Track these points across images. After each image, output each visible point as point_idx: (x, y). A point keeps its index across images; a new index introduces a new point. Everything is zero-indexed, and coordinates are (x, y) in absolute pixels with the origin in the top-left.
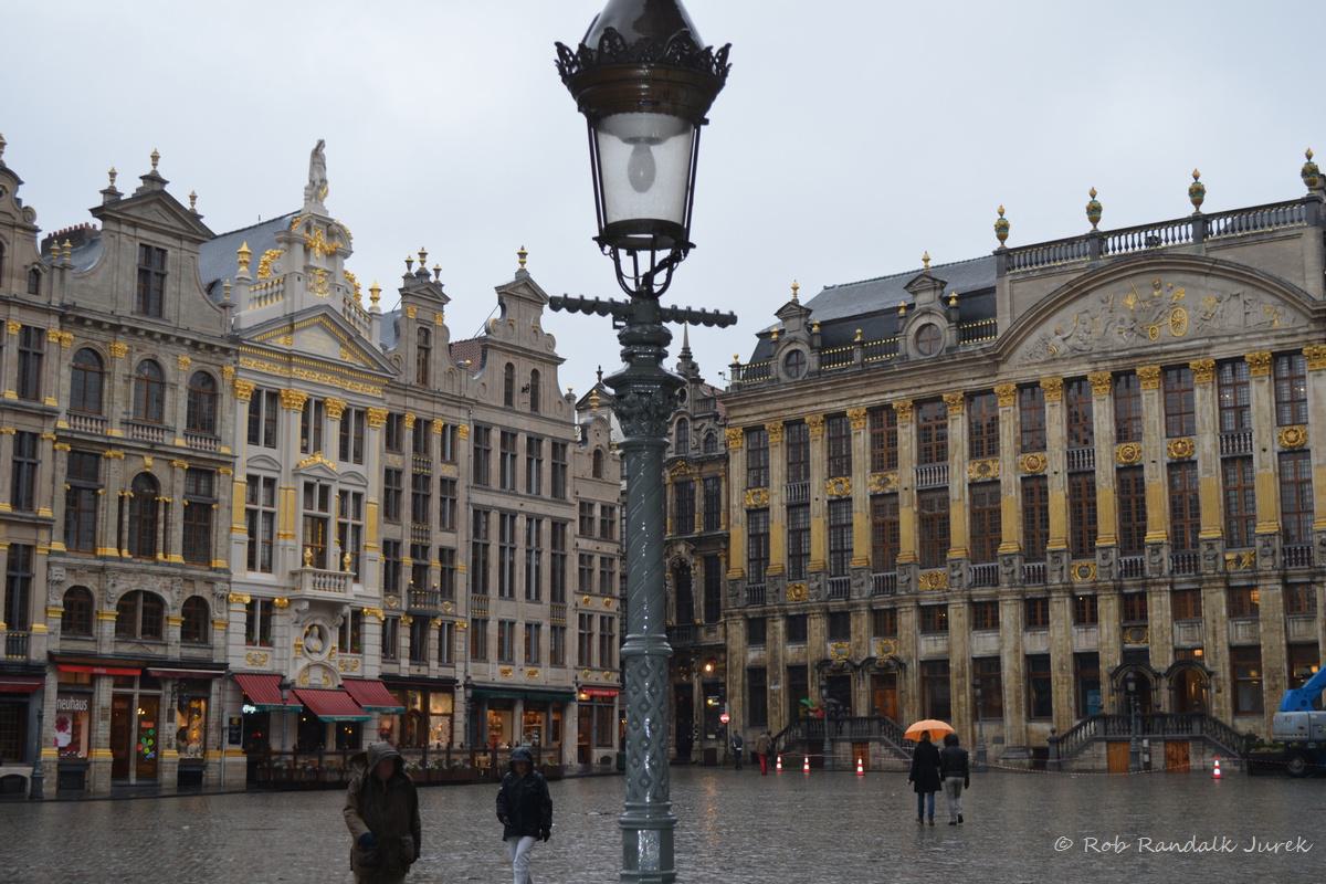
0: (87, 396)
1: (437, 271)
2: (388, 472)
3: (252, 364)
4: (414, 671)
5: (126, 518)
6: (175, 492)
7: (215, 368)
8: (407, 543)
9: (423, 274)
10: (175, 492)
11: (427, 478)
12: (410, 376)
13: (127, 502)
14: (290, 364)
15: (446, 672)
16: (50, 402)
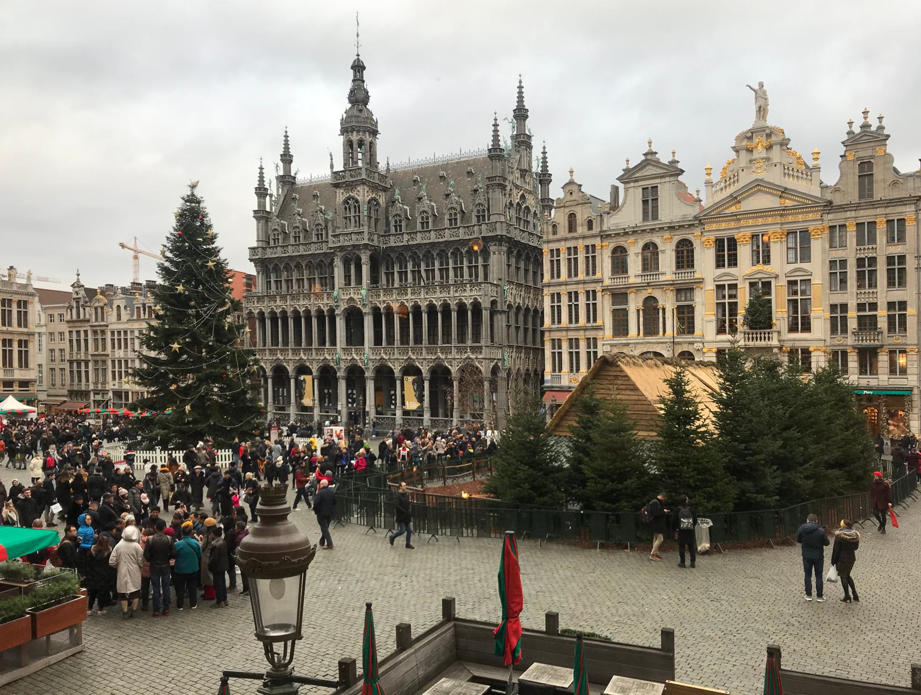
0: (620, 265)
1: (880, 118)
2: (832, 263)
3: (714, 226)
4: (863, 382)
5: (641, 319)
6: (668, 302)
7: (690, 236)
8: (852, 304)
9: (865, 126)
10: (668, 302)
11: (873, 261)
12: (854, 198)
13: (641, 313)
14: (739, 220)
15: (898, 382)
16: (598, 275)
